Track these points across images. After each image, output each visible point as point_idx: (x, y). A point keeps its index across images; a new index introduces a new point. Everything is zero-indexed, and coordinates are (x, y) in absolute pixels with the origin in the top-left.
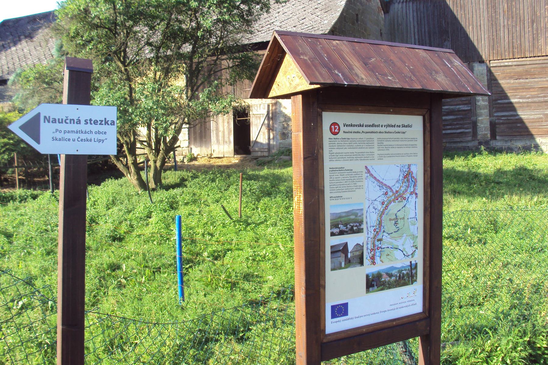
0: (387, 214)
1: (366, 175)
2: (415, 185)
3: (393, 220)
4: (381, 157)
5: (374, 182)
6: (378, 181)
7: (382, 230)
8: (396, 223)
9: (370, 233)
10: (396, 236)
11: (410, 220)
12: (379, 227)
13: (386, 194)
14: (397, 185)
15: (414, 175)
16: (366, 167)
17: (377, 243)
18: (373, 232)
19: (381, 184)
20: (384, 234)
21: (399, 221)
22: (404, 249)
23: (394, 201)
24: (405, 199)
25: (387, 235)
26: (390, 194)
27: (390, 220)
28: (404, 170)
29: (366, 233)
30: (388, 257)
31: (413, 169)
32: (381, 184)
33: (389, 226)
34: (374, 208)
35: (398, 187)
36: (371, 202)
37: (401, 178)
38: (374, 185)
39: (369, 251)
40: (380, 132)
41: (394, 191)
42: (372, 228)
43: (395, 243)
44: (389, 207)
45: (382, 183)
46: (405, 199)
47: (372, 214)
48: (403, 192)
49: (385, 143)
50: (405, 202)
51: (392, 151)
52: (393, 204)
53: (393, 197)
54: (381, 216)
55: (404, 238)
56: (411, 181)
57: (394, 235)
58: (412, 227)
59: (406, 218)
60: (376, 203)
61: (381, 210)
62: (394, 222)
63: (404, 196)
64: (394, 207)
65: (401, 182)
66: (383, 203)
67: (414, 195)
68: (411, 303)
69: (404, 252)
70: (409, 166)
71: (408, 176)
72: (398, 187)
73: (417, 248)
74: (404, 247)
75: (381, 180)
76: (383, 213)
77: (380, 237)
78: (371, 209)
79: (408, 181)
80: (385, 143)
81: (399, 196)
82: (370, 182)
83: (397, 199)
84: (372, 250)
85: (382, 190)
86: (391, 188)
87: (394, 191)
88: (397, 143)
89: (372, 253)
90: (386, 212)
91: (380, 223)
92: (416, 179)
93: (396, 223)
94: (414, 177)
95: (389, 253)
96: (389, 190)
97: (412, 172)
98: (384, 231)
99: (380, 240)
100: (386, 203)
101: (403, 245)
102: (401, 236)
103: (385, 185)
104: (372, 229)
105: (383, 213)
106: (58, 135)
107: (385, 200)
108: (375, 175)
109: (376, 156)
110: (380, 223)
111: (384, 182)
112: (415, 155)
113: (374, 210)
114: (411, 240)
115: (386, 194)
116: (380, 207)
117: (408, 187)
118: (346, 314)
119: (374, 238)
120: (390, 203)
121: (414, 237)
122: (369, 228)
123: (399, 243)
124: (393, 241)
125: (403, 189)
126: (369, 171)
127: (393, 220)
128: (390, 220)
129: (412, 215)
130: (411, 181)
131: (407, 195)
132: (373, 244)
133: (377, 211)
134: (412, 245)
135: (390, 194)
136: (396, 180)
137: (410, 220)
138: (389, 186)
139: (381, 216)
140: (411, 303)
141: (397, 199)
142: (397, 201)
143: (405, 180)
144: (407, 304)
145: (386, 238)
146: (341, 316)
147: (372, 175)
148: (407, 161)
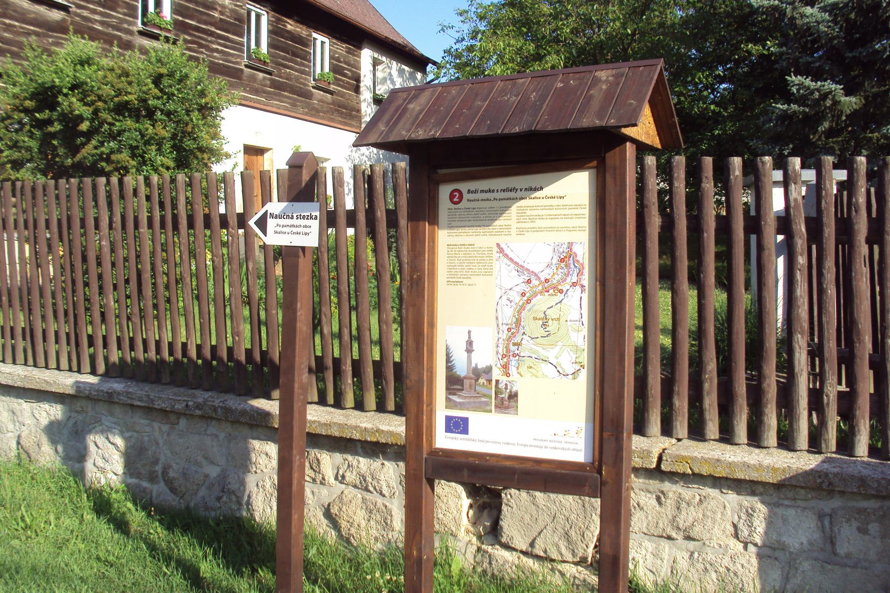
0: (529, 311)
1: (498, 255)
2: (580, 273)
3: (540, 319)
4: (521, 232)
6: (516, 263)
8: (544, 325)
9: (501, 332)
10: (545, 343)
11: (569, 323)
13: (529, 282)
14: (548, 271)
16: (498, 245)
17: (512, 348)
19: (520, 268)
20: (524, 336)
21: (550, 322)
24: (561, 291)
26: (535, 282)
27: (535, 319)
28: (561, 250)
32: (520, 268)
33: (532, 327)
34: (508, 299)
36: (503, 291)
37: (555, 261)
38: (509, 268)
39: (500, 357)
43: (543, 353)
46: (561, 291)
49: (529, 213)
50: (560, 296)
51: (539, 223)
52: (539, 297)
53: (540, 288)
54: (519, 313)
55: (558, 348)
59: (562, 320)
61: (521, 304)
62: (541, 322)
63: (560, 287)
64: (541, 303)
65: (554, 267)
66: (523, 295)
67: (578, 288)
68: (572, 446)
69: (559, 368)
70: (570, 245)
71: (566, 258)
75: (521, 263)
77: (517, 339)
78: (504, 300)
80: (529, 213)
82: (504, 266)
84: (504, 356)
86: (536, 275)
88: (548, 212)
89: (505, 360)
90: (528, 307)
91: (518, 322)
93: (544, 325)
94: (578, 261)
96: (533, 278)
97: (575, 253)
99: (518, 345)
100: (527, 295)
101: (557, 358)
102: (553, 345)
103: (527, 270)
105: (522, 308)
106: (279, 229)
108: (511, 255)
109: (514, 231)
110: (518, 322)
111: (526, 266)
113: (508, 303)
114: (572, 354)
115: (529, 282)
116: (517, 298)
117: (568, 275)
118: (465, 431)
119: (509, 339)
120: (535, 295)
122: (500, 325)
123: (551, 354)
124: (540, 349)
125: (557, 278)
126: (501, 250)
127: (540, 319)
128: (535, 319)
132: (507, 347)
134: (574, 360)
135: (536, 282)
136: (546, 265)
137: (569, 323)
138: (533, 272)
139: (519, 313)
140: (572, 446)
143: (563, 265)
144: (566, 446)
146: (458, 433)
147: (506, 256)
148: (565, 238)
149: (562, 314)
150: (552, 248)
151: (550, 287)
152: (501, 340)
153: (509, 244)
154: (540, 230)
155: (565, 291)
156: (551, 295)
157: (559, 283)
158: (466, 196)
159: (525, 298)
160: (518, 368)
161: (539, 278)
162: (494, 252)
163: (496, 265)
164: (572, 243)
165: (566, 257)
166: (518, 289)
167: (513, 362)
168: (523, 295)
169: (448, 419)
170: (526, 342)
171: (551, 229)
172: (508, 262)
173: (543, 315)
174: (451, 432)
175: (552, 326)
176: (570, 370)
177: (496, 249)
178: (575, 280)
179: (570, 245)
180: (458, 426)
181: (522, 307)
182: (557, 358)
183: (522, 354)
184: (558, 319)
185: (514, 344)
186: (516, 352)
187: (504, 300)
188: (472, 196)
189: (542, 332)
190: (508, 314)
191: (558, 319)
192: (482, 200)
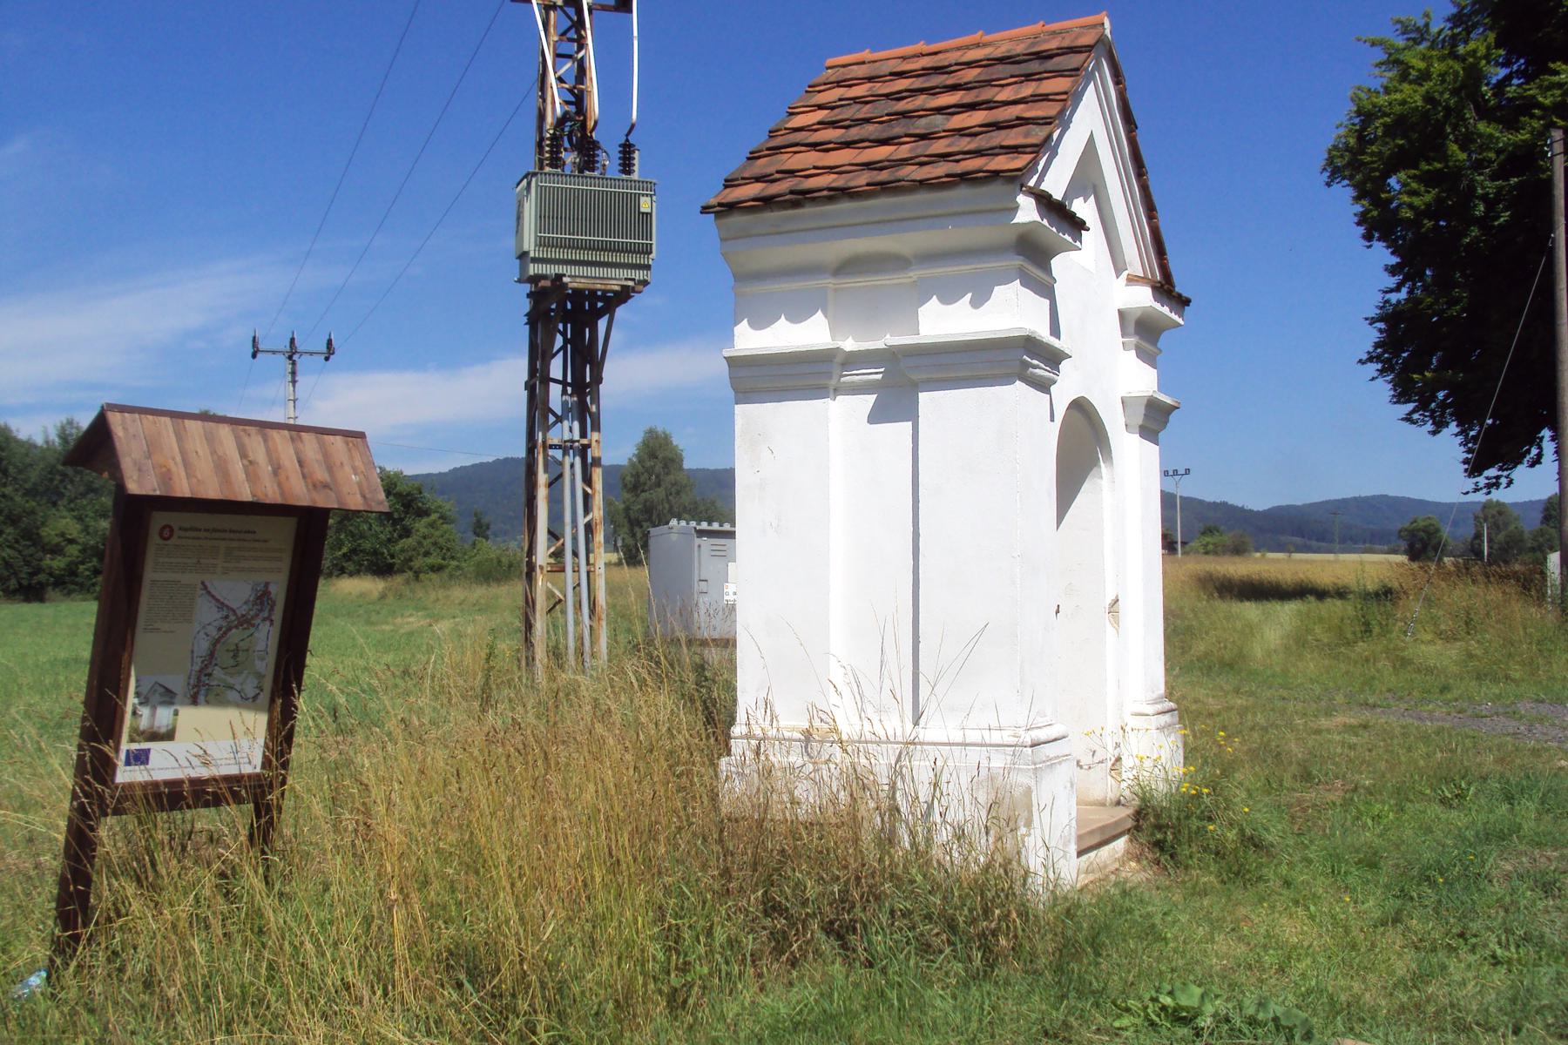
2: (272, 610)
8: (235, 656)
13: (227, 617)
19: (221, 605)
31: (273, 589)
32: (221, 605)
33: (224, 657)
43: (230, 680)
58: (257, 662)
64: (235, 635)
70: (267, 584)
71: (263, 598)
76: (217, 641)
78: (202, 634)
81: (245, 622)
93: (235, 656)
99: (209, 675)
102: (240, 673)
110: (212, 654)
117: (261, 610)
119: (201, 671)
120: (230, 629)
121: (260, 676)
126: (205, 587)
129: (261, 646)
132: (199, 679)
145: (217, 672)
170: (217, 672)
176: (251, 695)
180: (140, 758)
189: (232, 662)
190: (204, 646)
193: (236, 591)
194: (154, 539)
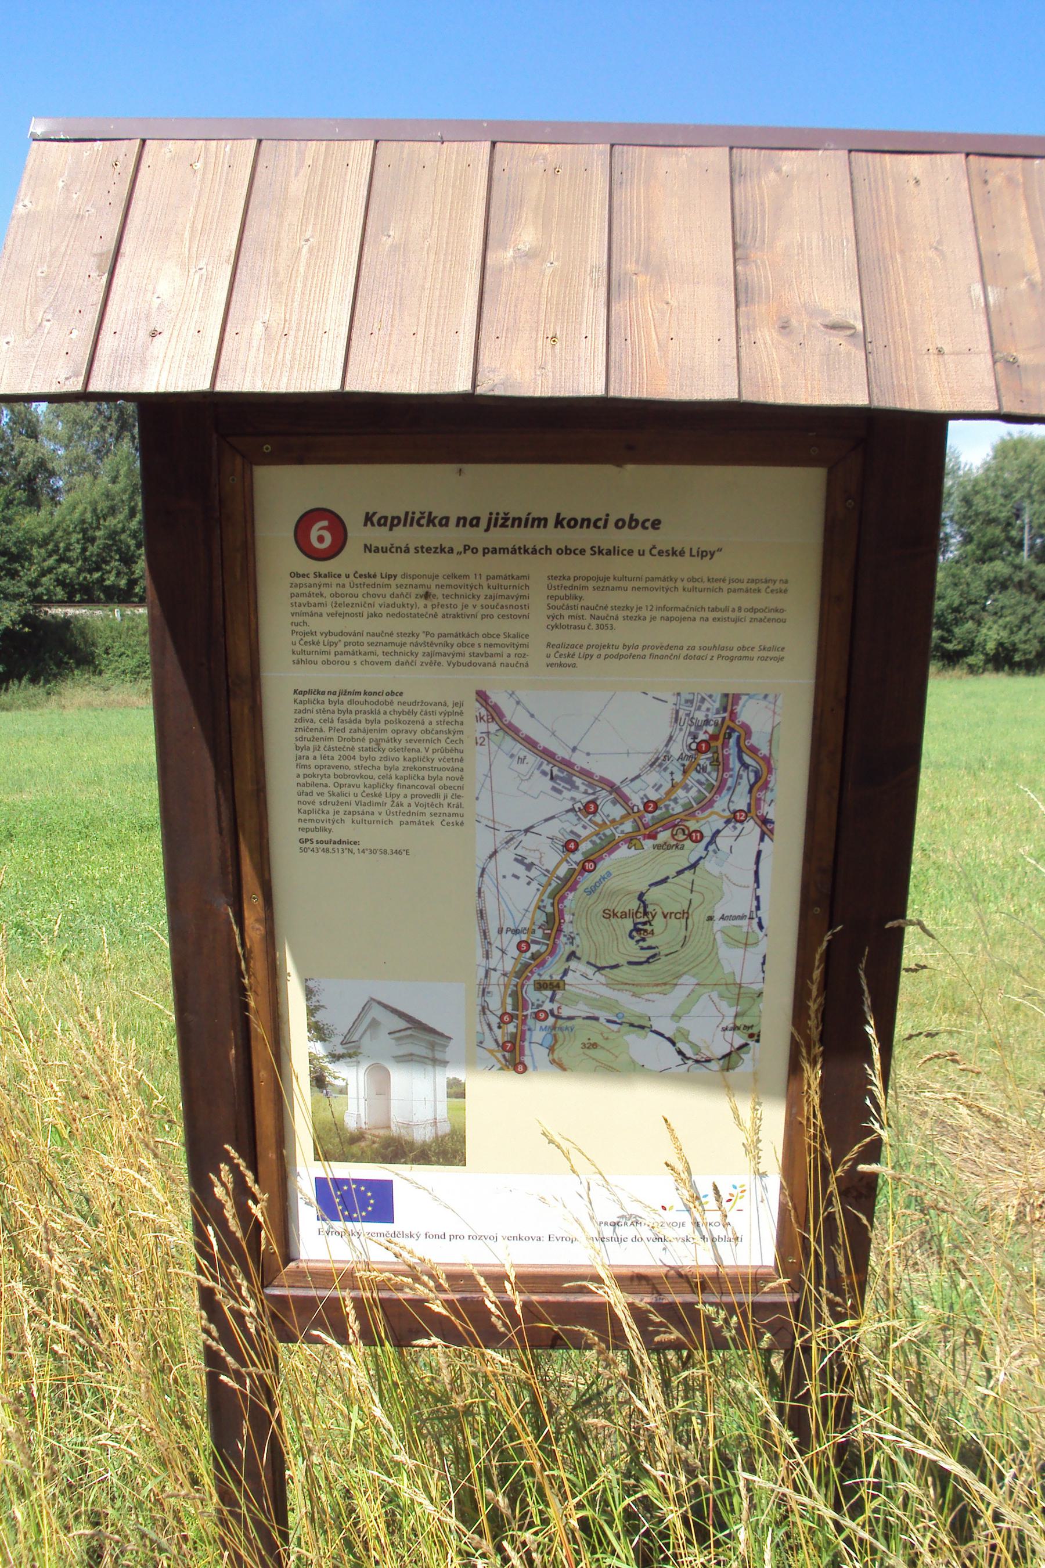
0: (590, 891)
1: (482, 727)
2: (760, 784)
3: (624, 915)
4: (563, 657)
5: (522, 760)
6: (548, 754)
7: (564, 949)
8: (639, 932)
9: (496, 954)
12: (547, 937)
13: (590, 808)
14: (653, 777)
15: (758, 740)
17: (532, 995)
18: (513, 951)
19: (562, 770)
20: (573, 964)
21: (658, 923)
22: (685, 1035)
23: (630, 840)
24: (696, 836)
25: (590, 971)
27: (610, 914)
28: (700, 716)
29: (479, 952)
30: (591, 1052)
31: (749, 713)
32: (562, 770)
34: (520, 860)
35: (657, 788)
36: (502, 836)
37: (676, 750)
38: (523, 768)
39: (495, 1021)
40: (567, 551)
41: (637, 801)
42: (507, 937)
44: (603, 867)
45: (568, 764)
46: (696, 836)
47: (509, 886)
48: (687, 807)
49: (591, 597)
50: (693, 851)
51: (623, 633)
52: (623, 851)
54: (558, 896)
55: (680, 993)
56: (734, 763)
57: (626, 973)
59: (697, 916)
60: (529, 840)
61: (562, 872)
62: (629, 924)
63: (692, 825)
64: (629, 869)
65: (675, 767)
66: (570, 846)
70: (730, 702)
71: (721, 743)
72: (657, 788)
73: (755, 1037)
74: (684, 1024)
75: (562, 753)
76: (569, 883)
77: (551, 971)
78: (506, 860)
79: (720, 764)
82: (502, 760)
83: (653, 836)
84: (505, 1019)
85: (567, 794)
86: (613, 788)
87: (637, 801)
88: (660, 598)
89: (511, 1028)
90: (587, 881)
91: (553, 923)
92: (767, 760)
93: (639, 932)
94: (754, 750)
95: (596, 1038)
96: (604, 797)
98: (572, 955)
99: (554, 986)
101: (676, 1017)
102: (666, 985)
103: (586, 774)
104: (511, 942)
105: (569, 883)
107: (584, 833)
108: (528, 728)
110: (553, 923)
111: (579, 760)
112: (772, 654)
113: (520, 870)
114: (724, 1005)
115: (590, 808)
116: (552, 859)
119: (522, 972)
120: (610, 846)
126: (495, 713)
127: (624, 915)
128: (610, 914)
130: (734, 763)
131: (708, 823)
133: (534, 873)
134: (729, 1022)
136: (650, 758)
137: (718, 924)
138: (602, 780)
141: (653, 836)
142: (648, 843)
143: (704, 760)
147: (511, 730)
148: (714, 680)
149: (696, 899)
150: (666, 712)
151: (653, 823)
152: (494, 976)
153: (521, 694)
154: (629, 653)
155: (708, 834)
156: (665, 846)
157: (690, 812)
158: (358, 534)
159: (578, 857)
160: (551, 1049)
161: (622, 798)
162: (469, 718)
163: (477, 760)
164: (736, 698)
165: (714, 737)
166: (553, 828)
167: (538, 1033)
168: (570, 846)
169: (321, 1183)
171: (665, 652)
172: (520, 750)
173: (635, 904)
174: (335, 1217)
175: (664, 934)
177: (474, 707)
178: (741, 802)
179: (730, 702)
181: (565, 880)
182: (676, 1017)
183: (565, 1012)
184: (685, 914)
185: (540, 986)
186: (547, 1006)
187: (506, 860)
188: (380, 536)
189: (632, 950)
190: (519, 900)
191: (685, 914)
192: (420, 549)
193: (625, 725)
194: (278, 558)
